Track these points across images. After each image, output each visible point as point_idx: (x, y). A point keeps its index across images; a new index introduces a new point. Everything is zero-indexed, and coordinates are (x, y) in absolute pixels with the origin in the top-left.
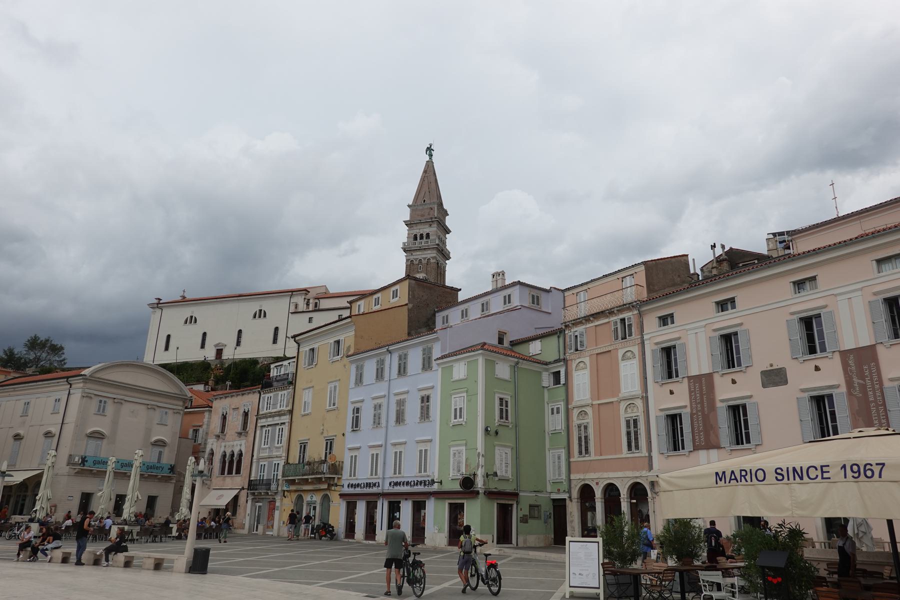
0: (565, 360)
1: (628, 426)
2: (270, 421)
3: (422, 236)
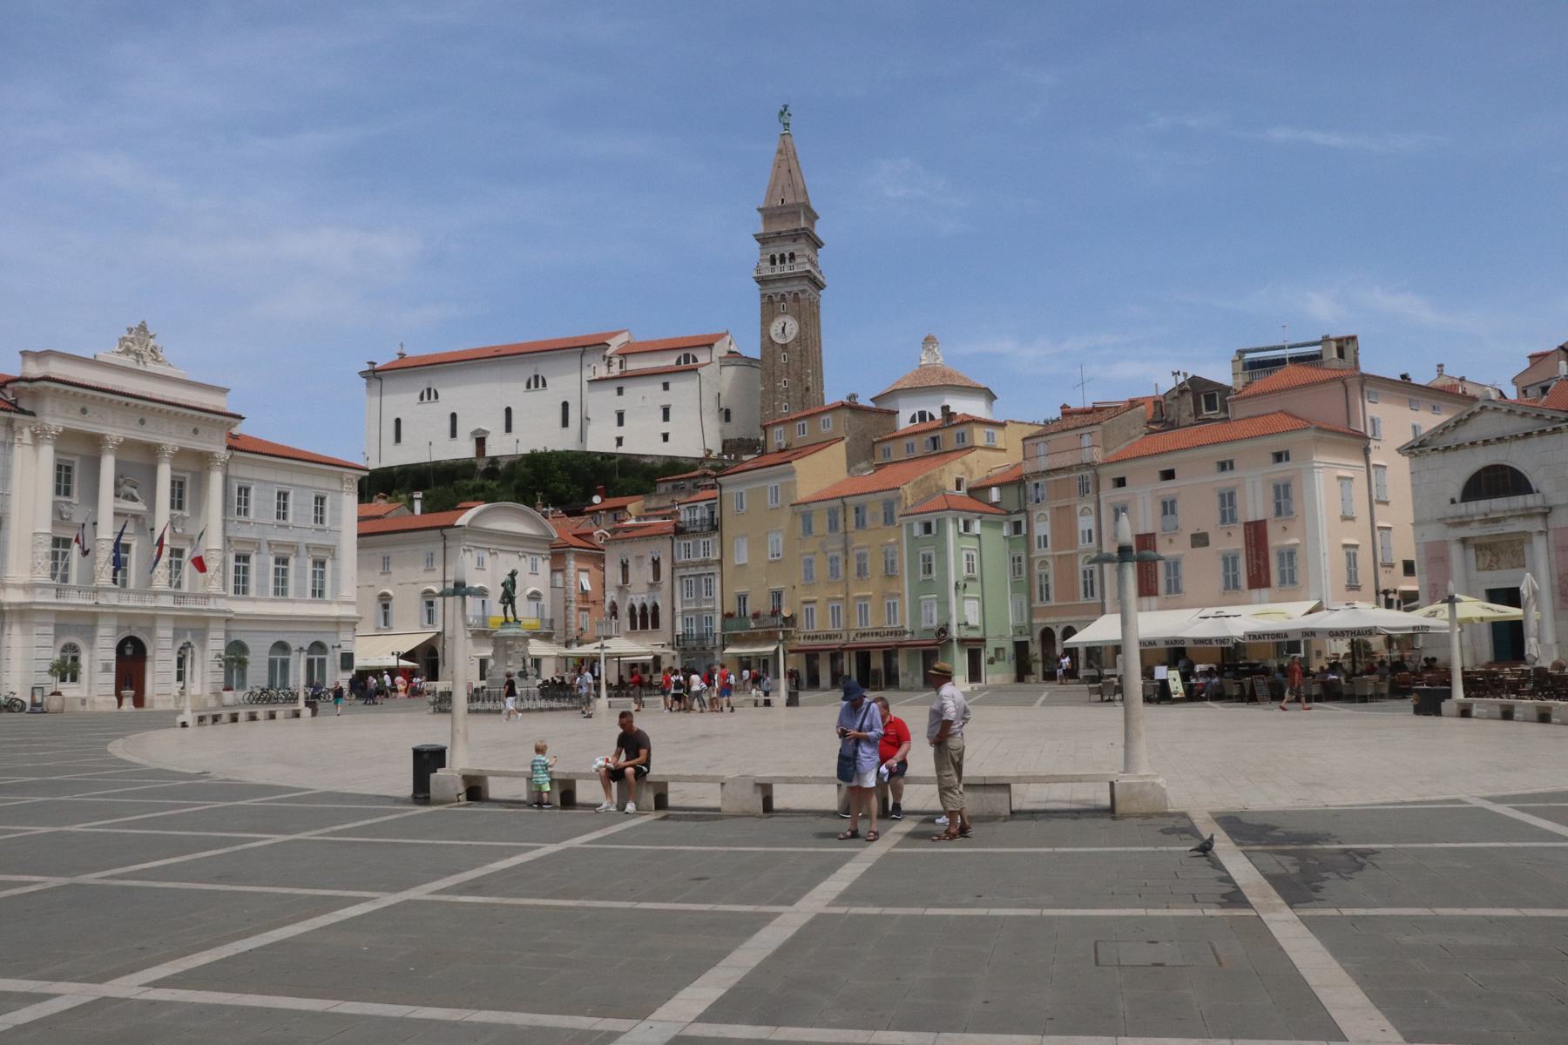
0: (1025, 511)
2: (692, 571)
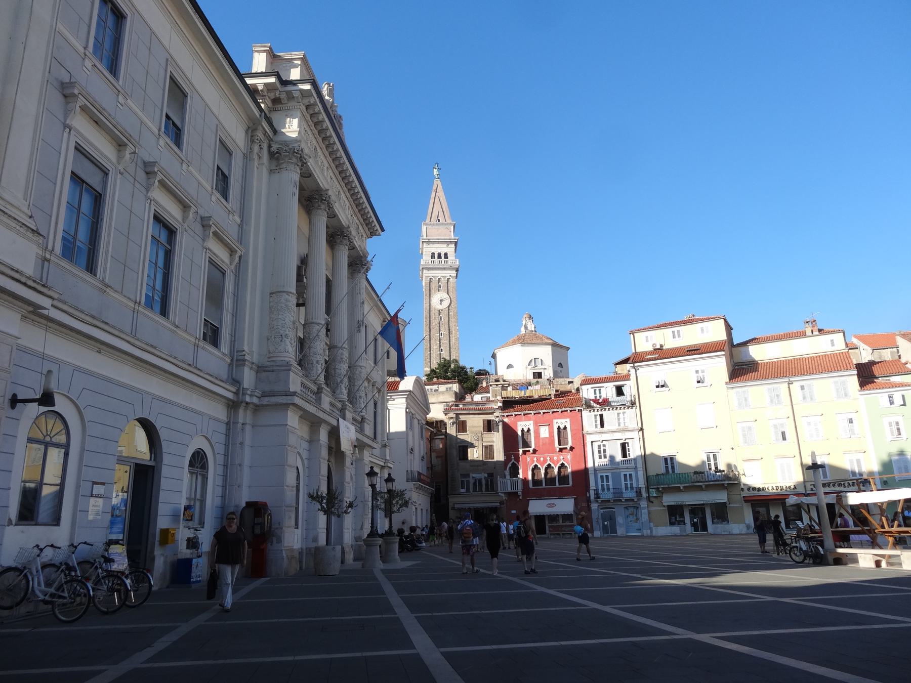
3: (439, 256)
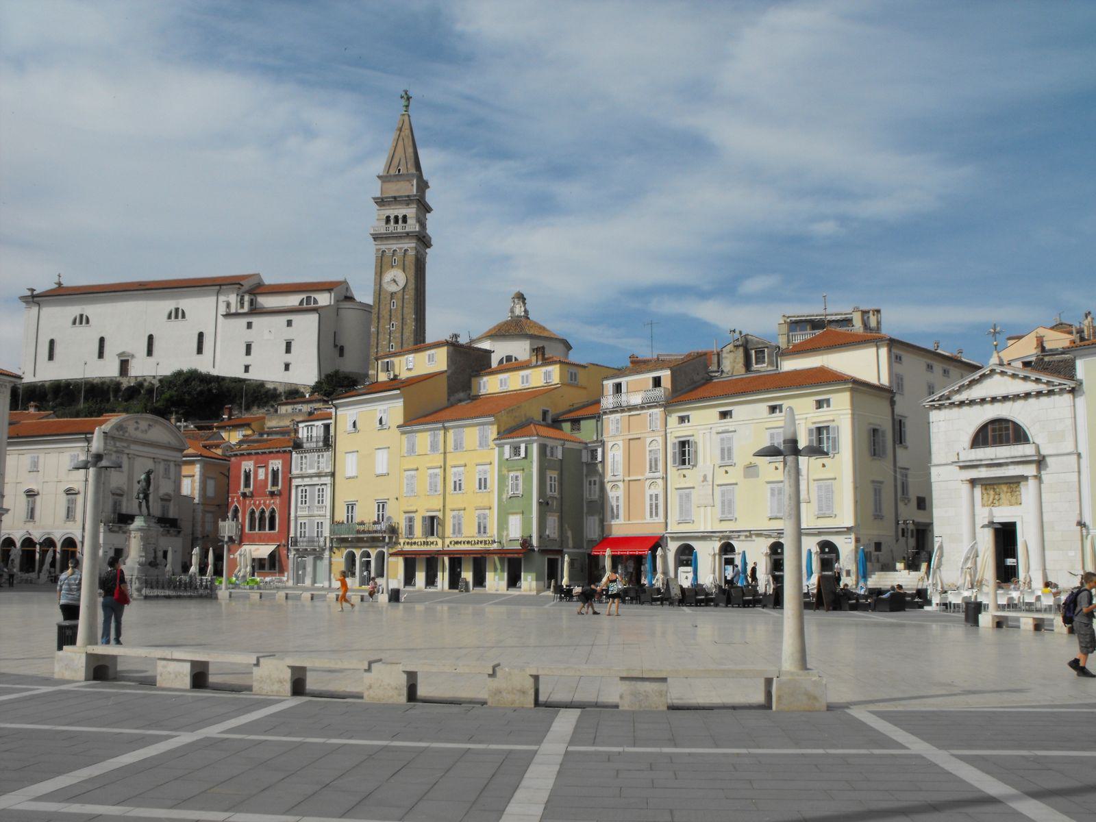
1: (651, 500)
2: (307, 481)
3: (396, 218)
